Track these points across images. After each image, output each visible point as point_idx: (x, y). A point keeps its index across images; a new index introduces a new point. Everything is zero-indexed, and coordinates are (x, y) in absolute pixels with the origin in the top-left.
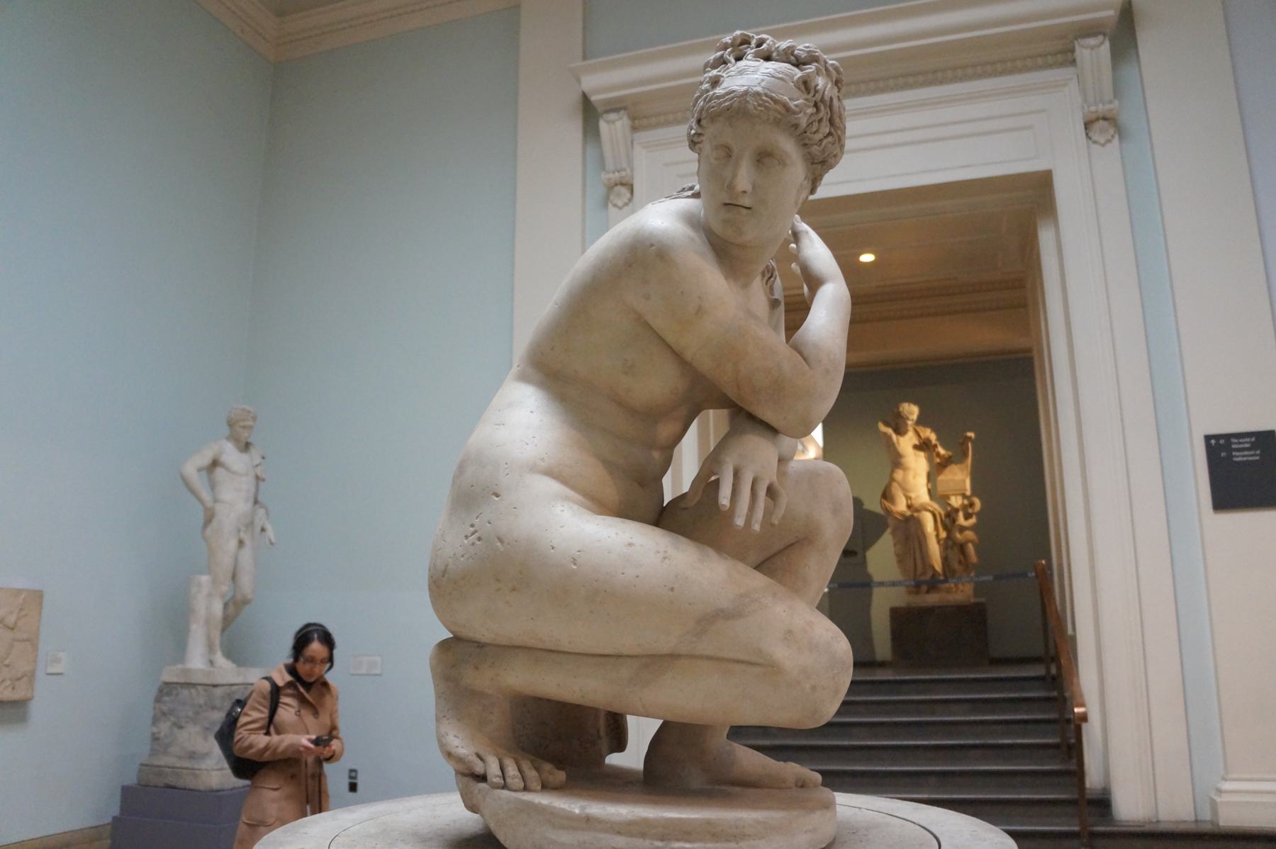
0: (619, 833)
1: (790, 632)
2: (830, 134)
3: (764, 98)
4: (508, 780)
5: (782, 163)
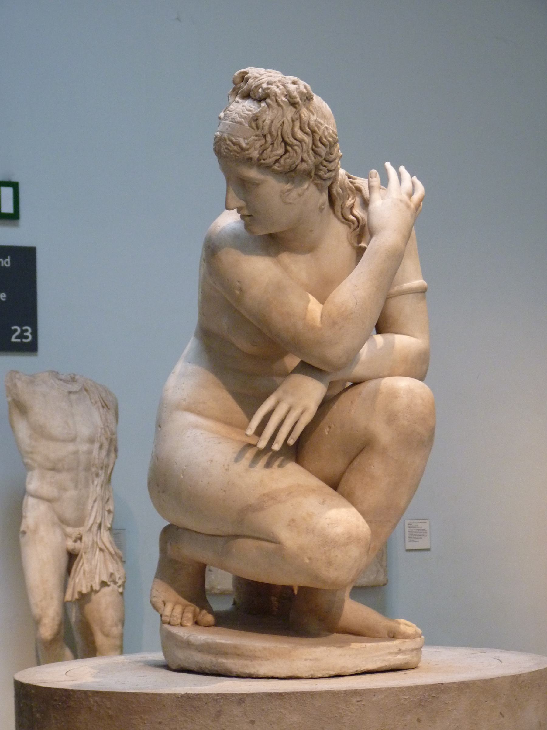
1: (293, 520)
2: (286, 151)
3: (228, 142)
5: (256, 184)
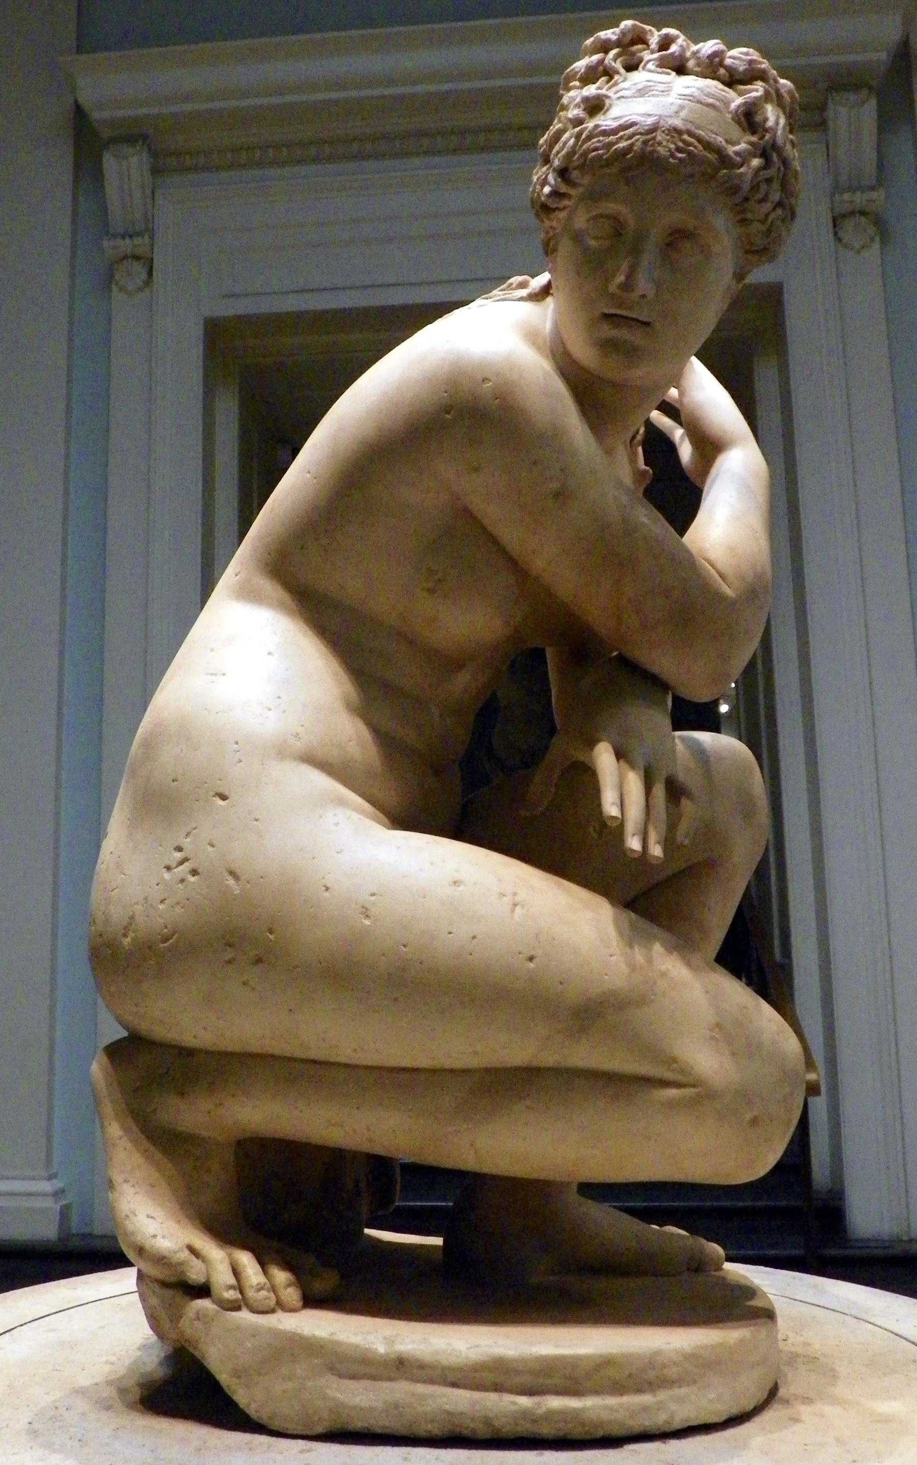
0: (454, 1385)
3: (686, 137)
4: (250, 1294)
